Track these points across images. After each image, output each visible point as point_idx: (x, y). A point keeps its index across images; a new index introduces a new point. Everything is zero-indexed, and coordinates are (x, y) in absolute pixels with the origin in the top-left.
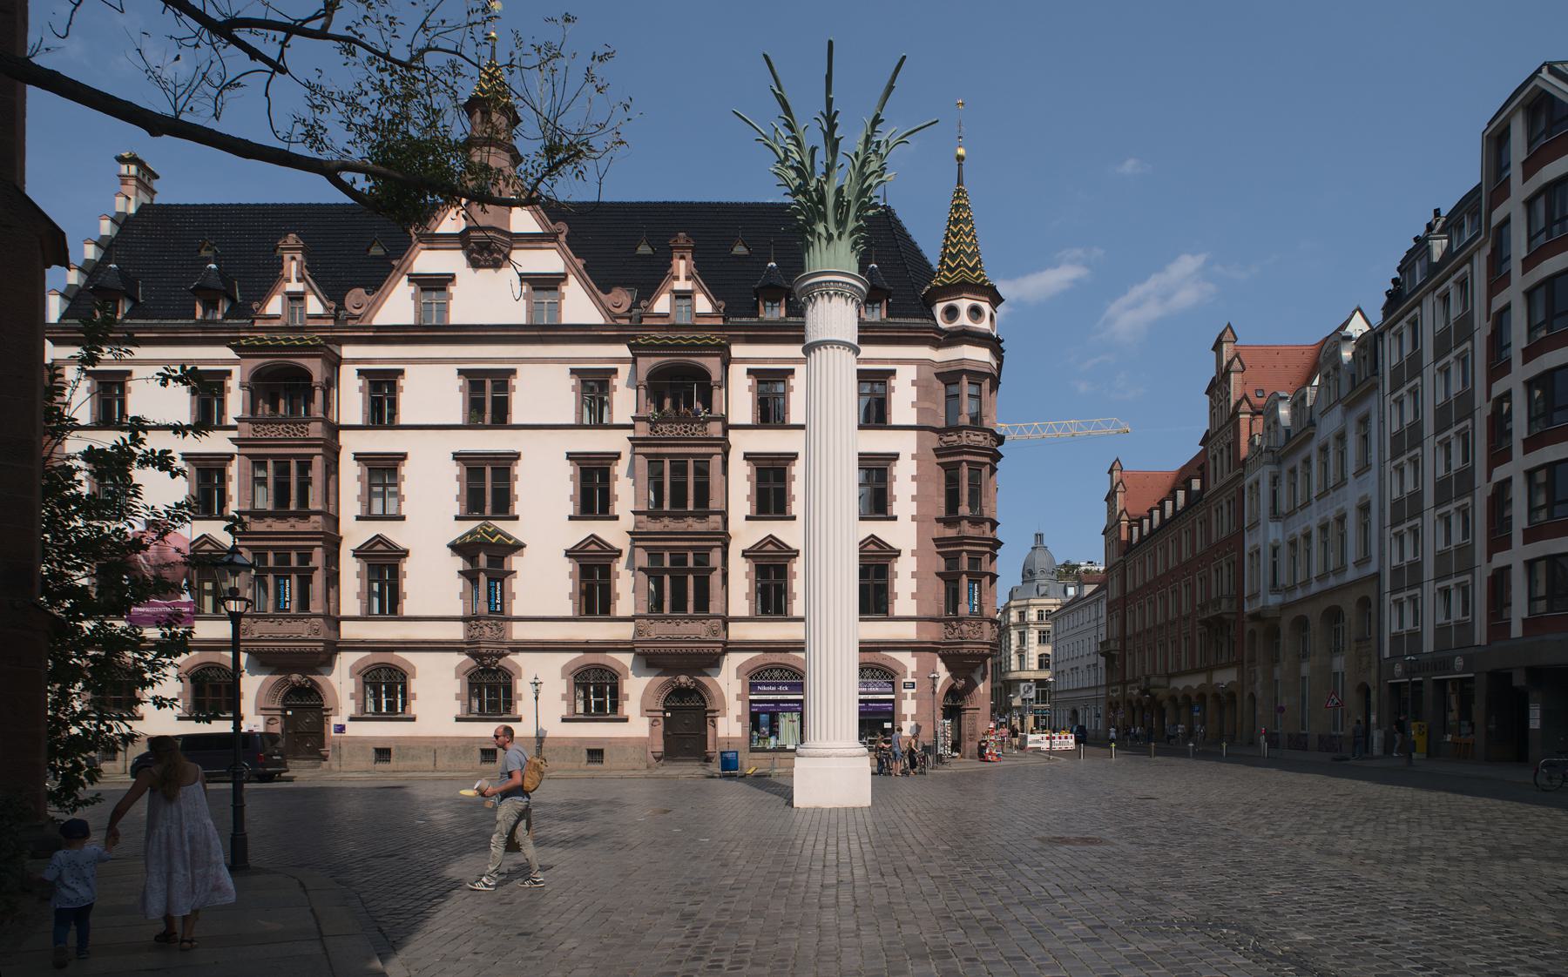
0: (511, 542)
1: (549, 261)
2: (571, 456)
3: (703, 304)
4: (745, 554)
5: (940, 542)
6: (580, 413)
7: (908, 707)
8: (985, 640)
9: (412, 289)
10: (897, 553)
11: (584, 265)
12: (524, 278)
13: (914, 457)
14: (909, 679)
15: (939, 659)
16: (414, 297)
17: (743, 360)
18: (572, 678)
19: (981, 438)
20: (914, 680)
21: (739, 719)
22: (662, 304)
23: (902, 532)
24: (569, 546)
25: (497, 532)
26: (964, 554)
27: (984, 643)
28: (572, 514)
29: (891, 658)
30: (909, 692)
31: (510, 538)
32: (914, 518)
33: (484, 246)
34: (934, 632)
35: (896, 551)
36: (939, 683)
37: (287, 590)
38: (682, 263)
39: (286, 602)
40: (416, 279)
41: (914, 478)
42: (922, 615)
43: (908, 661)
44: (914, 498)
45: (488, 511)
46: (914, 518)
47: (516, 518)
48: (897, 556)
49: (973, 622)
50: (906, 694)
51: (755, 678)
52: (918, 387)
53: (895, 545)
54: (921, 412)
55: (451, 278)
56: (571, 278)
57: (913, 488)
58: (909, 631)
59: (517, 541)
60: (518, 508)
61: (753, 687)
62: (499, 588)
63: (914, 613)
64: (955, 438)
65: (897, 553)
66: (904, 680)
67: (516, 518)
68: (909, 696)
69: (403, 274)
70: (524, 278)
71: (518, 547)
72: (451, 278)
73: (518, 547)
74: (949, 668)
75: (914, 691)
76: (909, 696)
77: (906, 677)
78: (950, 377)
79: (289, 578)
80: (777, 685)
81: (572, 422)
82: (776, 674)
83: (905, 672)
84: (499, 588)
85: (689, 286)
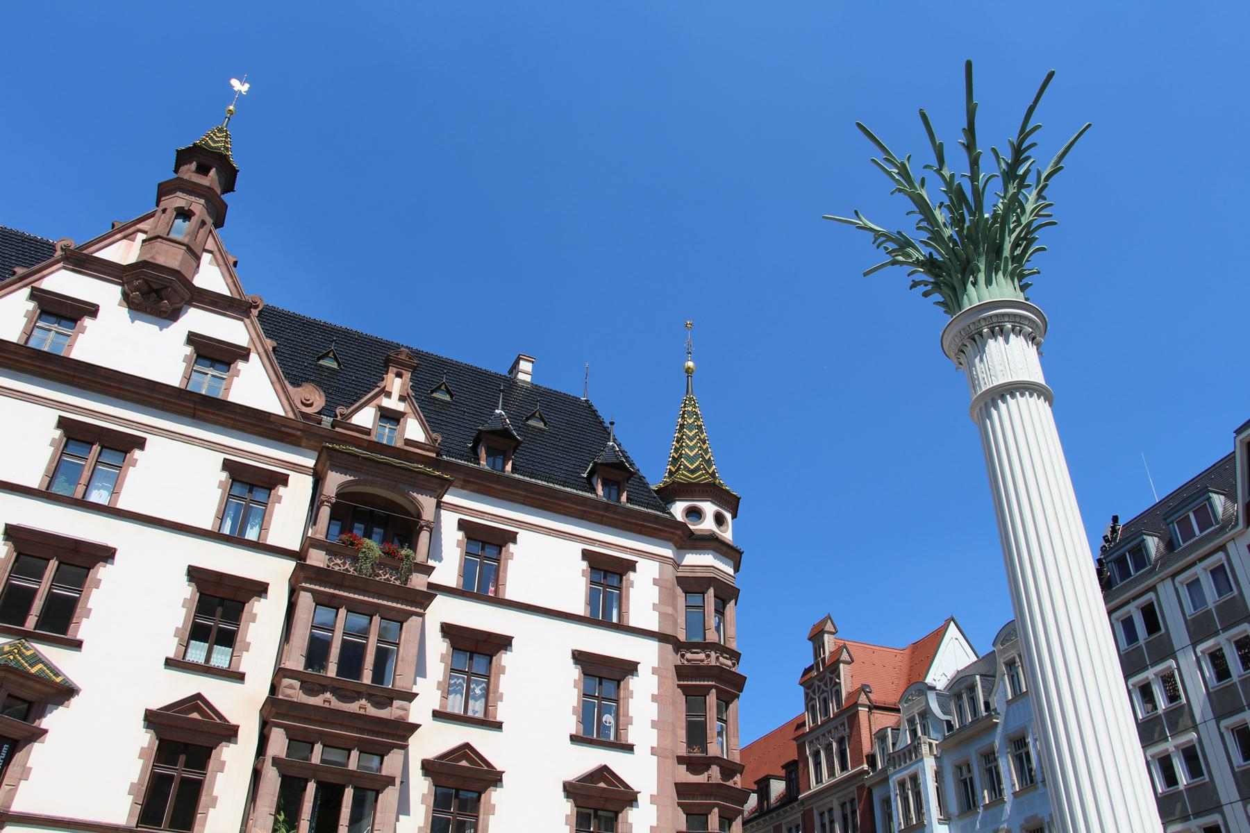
0: (58, 680)
1: (232, 331)
2: (195, 574)
3: (414, 430)
4: (428, 767)
5: (682, 790)
6: (221, 518)
9: (31, 305)
10: (629, 798)
11: (274, 349)
12: (194, 339)
13: (654, 671)
16: (28, 314)
17: (455, 508)
22: (365, 417)
24: (156, 705)
25: (37, 659)
26: (716, 810)
28: (172, 655)
31: (57, 674)
32: (654, 751)
33: (155, 286)
38: (398, 381)
40: (37, 295)
41: (654, 698)
44: (654, 724)
45: (31, 623)
46: (654, 751)
47: (77, 645)
52: (661, 588)
54: (663, 616)
55: (92, 310)
56: (254, 356)
57: (652, 711)
59: (66, 680)
60: (84, 629)
64: (702, 656)
65: (629, 798)
67: (77, 645)
69: (25, 286)
70: (194, 339)
71: (66, 692)
72: (92, 310)
73: (66, 692)
78: (692, 585)
81: (208, 527)
85: (401, 407)
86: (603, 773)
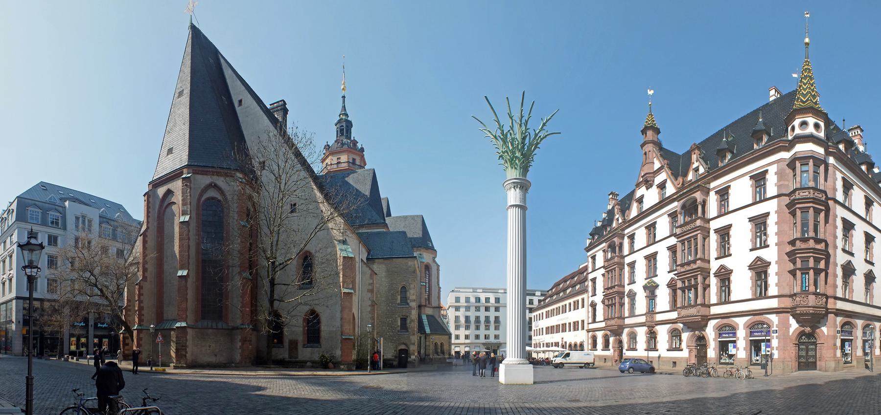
7: (775, 343)
8: (810, 305)
10: (770, 263)
14: (775, 328)
15: (791, 318)
18: (670, 334)
19: (801, 194)
20: (777, 329)
21: (714, 349)
23: (771, 254)
27: (809, 307)
29: (767, 318)
30: (775, 335)
34: (788, 303)
35: (768, 262)
36: (792, 330)
37: (807, 280)
39: (806, 286)
42: (780, 294)
43: (774, 318)
48: (769, 265)
49: (803, 296)
50: (773, 336)
51: (720, 330)
53: (769, 260)
58: (773, 303)
61: (720, 335)
62: (807, 278)
63: (776, 294)
65: (770, 263)
66: (773, 329)
68: (775, 337)
74: (798, 322)
75: (777, 334)
76: (775, 337)
77: (773, 328)
79: (808, 273)
80: (729, 333)
82: (727, 328)
83: (773, 324)
84: (807, 278)
86: (759, 259)
